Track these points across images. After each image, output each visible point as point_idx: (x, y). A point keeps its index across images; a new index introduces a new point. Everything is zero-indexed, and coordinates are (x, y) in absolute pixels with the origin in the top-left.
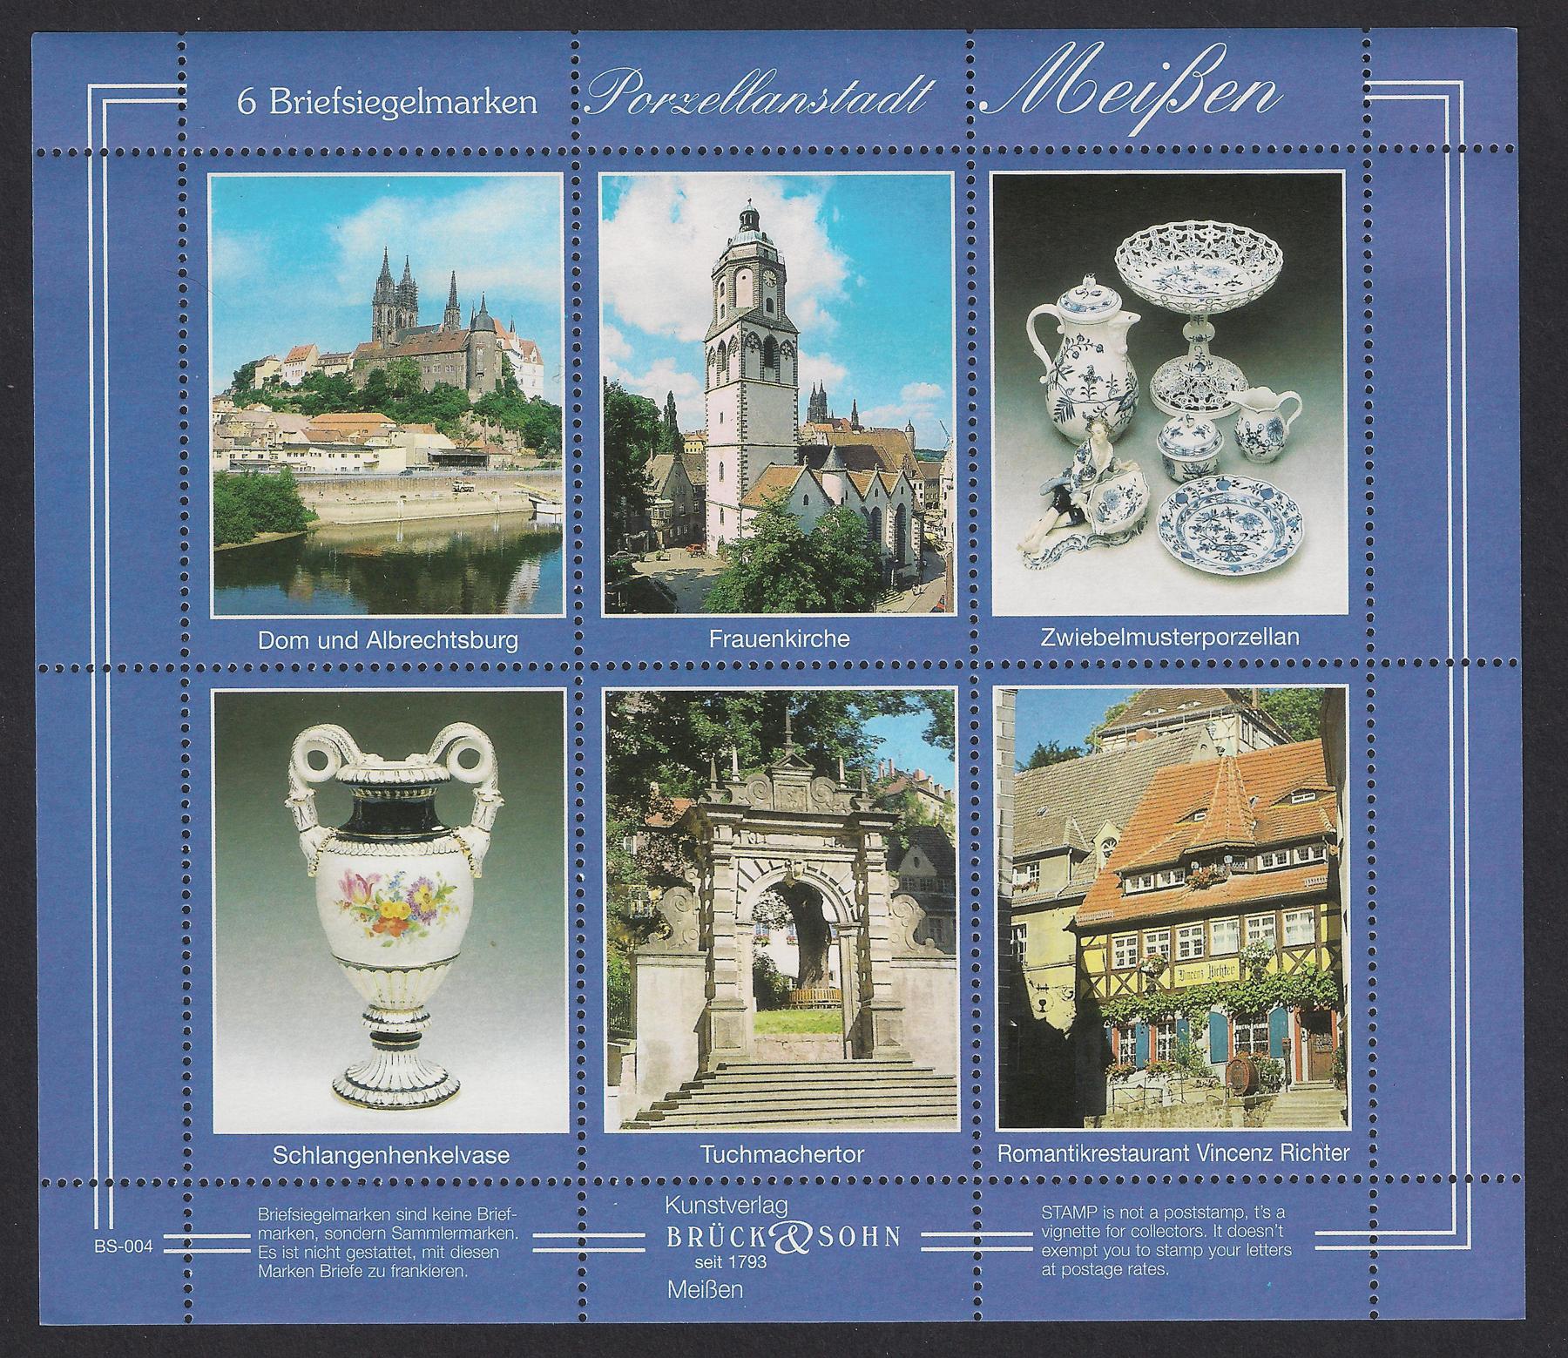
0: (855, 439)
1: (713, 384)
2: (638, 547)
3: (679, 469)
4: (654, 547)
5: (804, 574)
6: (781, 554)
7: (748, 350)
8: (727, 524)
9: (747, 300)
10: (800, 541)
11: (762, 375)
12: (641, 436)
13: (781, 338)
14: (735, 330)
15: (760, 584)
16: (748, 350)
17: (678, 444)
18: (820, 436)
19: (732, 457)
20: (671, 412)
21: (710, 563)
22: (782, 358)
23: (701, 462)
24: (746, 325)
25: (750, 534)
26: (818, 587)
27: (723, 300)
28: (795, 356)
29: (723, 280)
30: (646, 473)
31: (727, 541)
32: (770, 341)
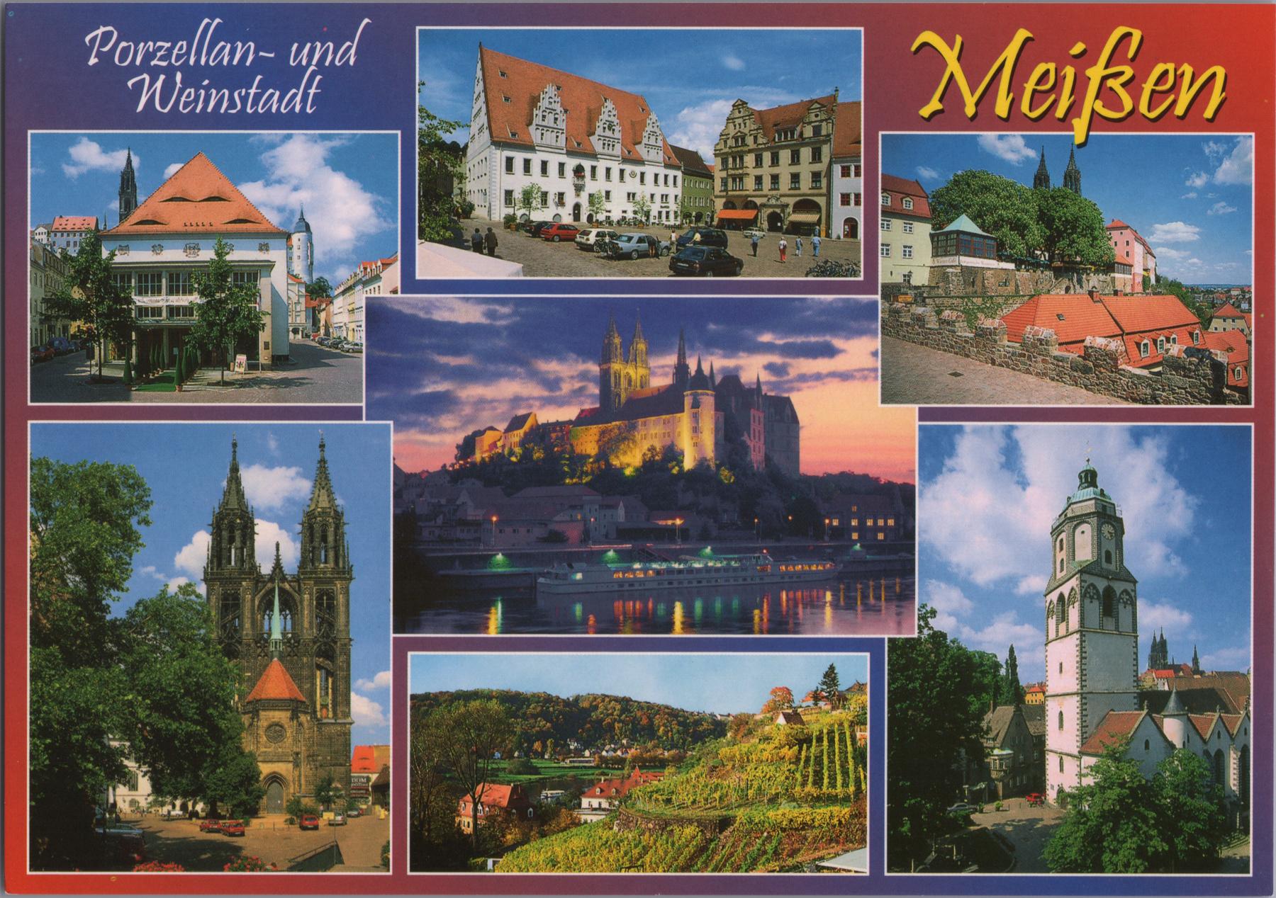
0: (1197, 682)
1: (1052, 635)
2: (978, 799)
3: (1019, 722)
4: (993, 797)
5: (1145, 819)
6: (1121, 800)
8: (1067, 770)
9: (1085, 552)
10: (1140, 786)
12: (980, 689)
13: (1119, 587)
14: (1074, 582)
15: (1100, 831)
16: (1087, 601)
17: (1018, 695)
18: (1160, 682)
19: (1071, 707)
20: (1012, 663)
21: (1049, 811)
22: (1121, 607)
23: (1041, 710)
24: (1086, 577)
25: (1089, 781)
26: (1160, 833)
27: (1062, 555)
28: (1134, 605)
29: (1063, 536)
30: (984, 725)
31: (1067, 790)
32: (1109, 591)
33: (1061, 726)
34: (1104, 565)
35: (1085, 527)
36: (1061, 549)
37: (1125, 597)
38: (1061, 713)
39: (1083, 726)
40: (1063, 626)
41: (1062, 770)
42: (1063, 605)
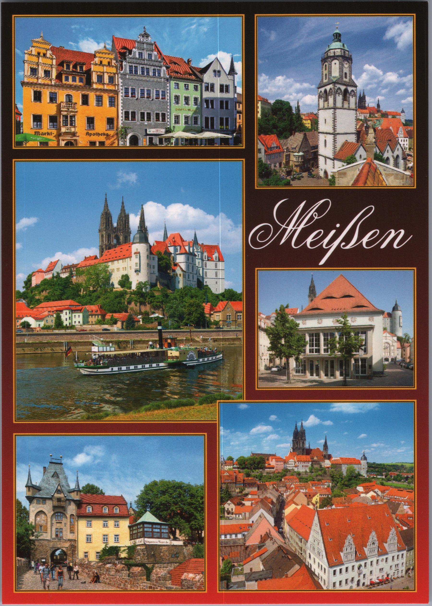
1: (321, 106)
7: (337, 95)
13: (350, 89)
16: (337, 95)
19: (330, 138)
22: (351, 97)
32: (346, 91)
33: (325, 146)
34: (344, 79)
35: (336, 61)
36: (326, 69)
37: (353, 93)
38: (325, 140)
39: (335, 147)
41: (326, 164)
42: (326, 95)
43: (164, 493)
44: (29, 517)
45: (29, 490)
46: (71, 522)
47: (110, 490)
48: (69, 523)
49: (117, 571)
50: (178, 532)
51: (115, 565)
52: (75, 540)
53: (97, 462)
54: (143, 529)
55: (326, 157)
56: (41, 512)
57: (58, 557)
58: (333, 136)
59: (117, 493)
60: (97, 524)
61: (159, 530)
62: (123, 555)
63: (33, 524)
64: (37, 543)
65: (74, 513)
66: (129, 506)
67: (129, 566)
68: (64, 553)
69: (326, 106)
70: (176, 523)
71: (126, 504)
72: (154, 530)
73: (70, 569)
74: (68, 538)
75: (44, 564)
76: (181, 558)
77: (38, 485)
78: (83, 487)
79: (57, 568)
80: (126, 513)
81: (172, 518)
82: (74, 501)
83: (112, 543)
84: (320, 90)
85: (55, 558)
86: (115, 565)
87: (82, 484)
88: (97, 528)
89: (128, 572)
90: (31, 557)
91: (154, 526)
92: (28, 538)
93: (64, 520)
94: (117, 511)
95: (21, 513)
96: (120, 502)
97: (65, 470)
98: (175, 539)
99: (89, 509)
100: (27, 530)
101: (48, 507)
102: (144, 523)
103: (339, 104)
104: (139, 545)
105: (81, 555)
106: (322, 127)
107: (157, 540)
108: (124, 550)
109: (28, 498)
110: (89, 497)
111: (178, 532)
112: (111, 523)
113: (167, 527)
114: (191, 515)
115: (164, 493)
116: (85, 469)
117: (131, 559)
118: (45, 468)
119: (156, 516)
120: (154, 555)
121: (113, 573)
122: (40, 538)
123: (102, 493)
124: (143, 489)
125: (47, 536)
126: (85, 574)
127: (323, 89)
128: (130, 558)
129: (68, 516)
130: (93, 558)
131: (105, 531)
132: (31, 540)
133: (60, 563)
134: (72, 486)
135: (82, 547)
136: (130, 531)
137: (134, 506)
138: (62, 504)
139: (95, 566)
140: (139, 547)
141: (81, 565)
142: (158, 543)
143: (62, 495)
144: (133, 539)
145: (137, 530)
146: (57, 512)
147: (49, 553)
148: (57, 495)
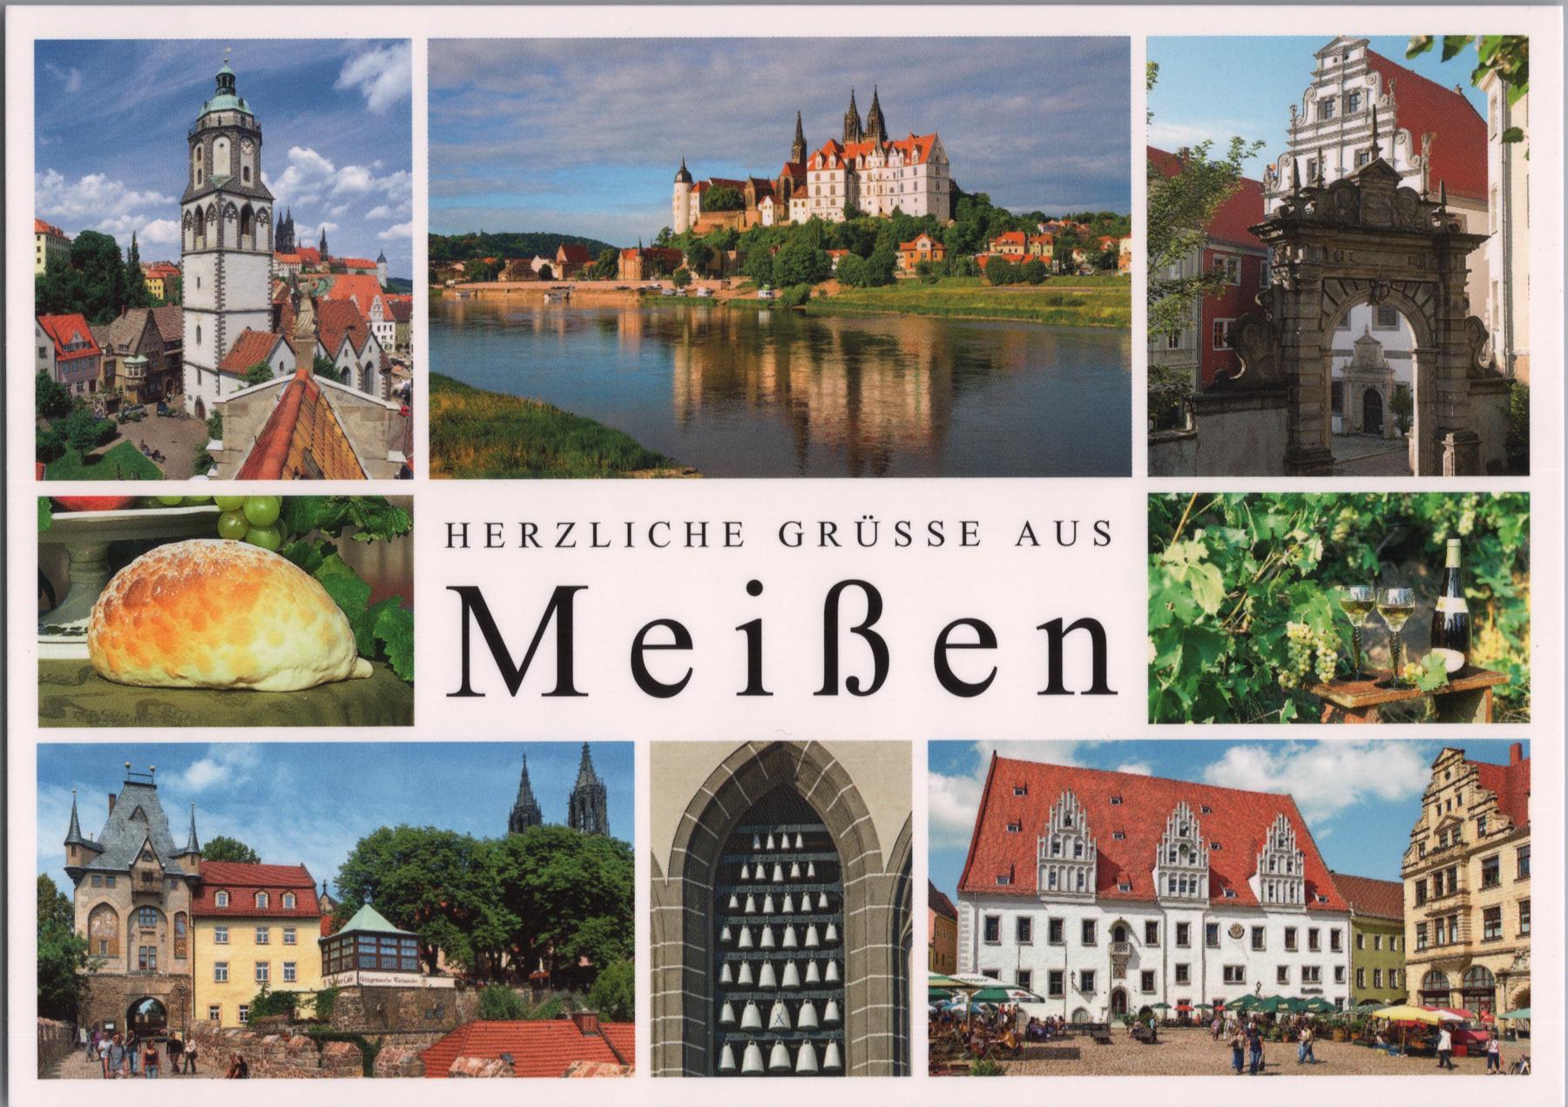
1: (189, 246)
11: (239, 244)
13: (256, 206)
19: (209, 322)
32: (247, 210)
33: (199, 340)
34: (244, 183)
37: (263, 216)
38: (199, 329)
40: (200, 239)
41: (200, 382)
42: (201, 220)
43: (405, 857)
44: (73, 918)
45: (73, 854)
46: (176, 931)
47: (273, 852)
48: (171, 935)
49: (292, 1052)
50: (441, 955)
51: (285, 1037)
52: (187, 976)
53: (240, 781)
54: (356, 949)
55: (199, 368)
56: (104, 906)
57: (146, 1019)
58: (214, 317)
59: (290, 860)
60: (242, 935)
61: (394, 952)
62: (306, 1013)
63: (85, 937)
64: (93, 984)
65: (186, 908)
66: (320, 890)
67: (320, 1040)
68: (159, 1009)
69: (200, 247)
70: (437, 933)
71: (313, 887)
72: (383, 951)
73: (176, 1048)
74: (170, 971)
75: (110, 1034)
76: (448, 1021)
77: (95, 840)
78: (207, 846)
79: (144, 1046)
80: (314, 909)
81: (426, 919)
82: (187, 879)
83: (278, 984)
84: (186, 207)
85: (137, 1019)
86: (285, 1037)
87: (205, 838)
88: (241, 946)
89: (317, 1055)
90: (79, 1018)
91: (383, 941)
92: (72, 971)
93: (160, 928)
94: (289, 902)
95: (54, 910)
96: (298, 880)
97: (163, 803)
98: (435, 972)
99: (221, 900)
100: (68, 951)
101: (119, 895)
102: (356, 934)
103: (230, 241)
104: (346, 988)
105: (201, 1012)
106: (191, 297)
107: (391, 976)
108: (308, 1002)
109: (71, 872)
110: (218, 872)
111: (441, 955)
112: (276, 932)
113: (414, 943)
114: (476, 912)
115: (405, 857)
116: (212, 800)
117: (327, 1021)
118: (112, 796)
119: (387, 916)
120: (381, 1013)
121: (281, 1057)
122: (99, 971)
123: (253, 859)
124: (354, 848)
125: (117, 966)
126: (211, 1061)
127: (192, 207)
128: (322, 1020)
129: (170, 916)
130: (231, 1019)
131: (262, 953)
132: (77, 977)
133: (151, 1034)
134: (181, 841)
135: (206, 993)
136: (323, 953)
137: (333, 892)
138: (157, 886)
139: (238, 1039)
140: (344, 994)
141: (202, 1038)
142: (393, 984)
143: (153, 866)
144: (329, 973)
145: (340, 949)
146: (145, 907)
147: (124, 1008)
148: (142, 865)
